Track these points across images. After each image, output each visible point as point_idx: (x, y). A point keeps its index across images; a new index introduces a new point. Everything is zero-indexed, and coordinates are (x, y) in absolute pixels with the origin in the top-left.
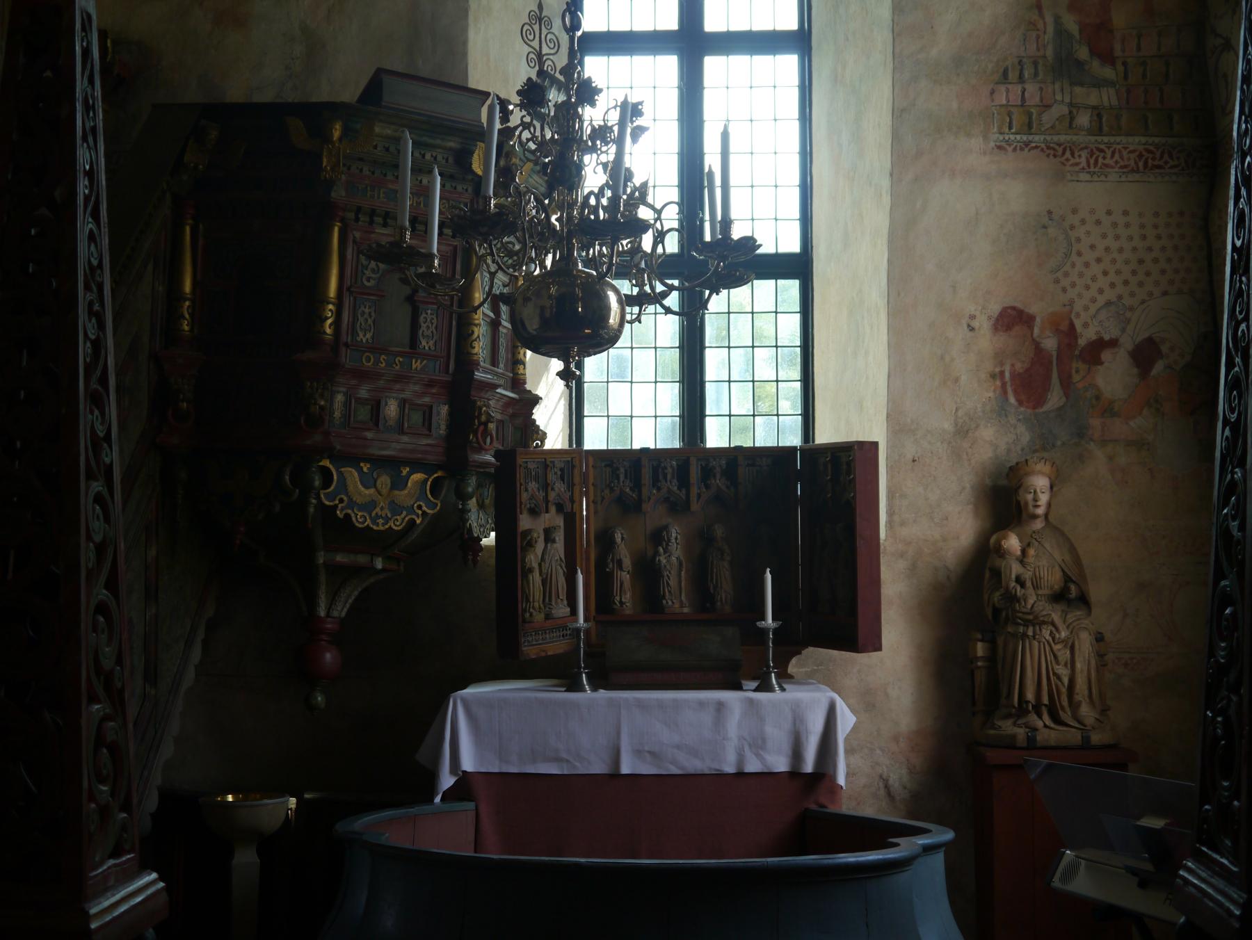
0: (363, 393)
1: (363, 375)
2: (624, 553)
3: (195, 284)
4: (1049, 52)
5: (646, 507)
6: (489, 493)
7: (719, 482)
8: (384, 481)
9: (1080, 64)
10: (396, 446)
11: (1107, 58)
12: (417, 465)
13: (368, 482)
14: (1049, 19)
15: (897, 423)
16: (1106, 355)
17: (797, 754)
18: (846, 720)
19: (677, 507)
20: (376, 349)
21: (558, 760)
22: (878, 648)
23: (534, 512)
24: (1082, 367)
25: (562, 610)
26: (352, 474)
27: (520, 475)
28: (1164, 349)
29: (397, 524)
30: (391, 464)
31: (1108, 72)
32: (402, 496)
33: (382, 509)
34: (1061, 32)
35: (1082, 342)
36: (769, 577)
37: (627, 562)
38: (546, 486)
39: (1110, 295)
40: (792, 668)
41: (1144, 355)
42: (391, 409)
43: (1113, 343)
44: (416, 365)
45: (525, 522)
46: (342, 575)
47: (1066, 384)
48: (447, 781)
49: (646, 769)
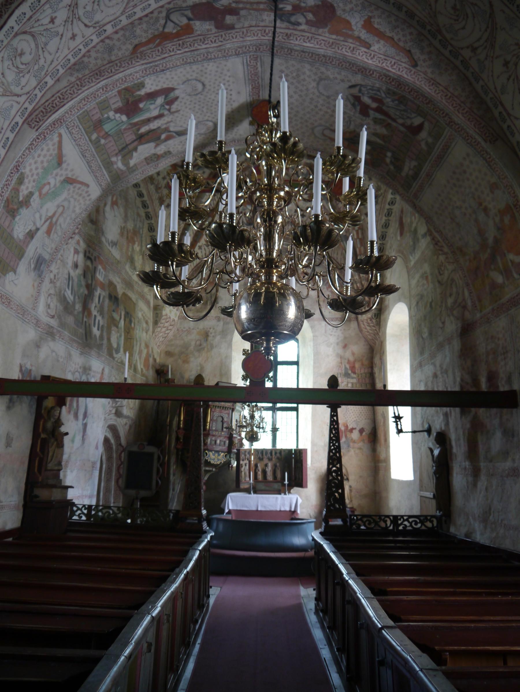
0: (213, 439)
1: (213, 436)
2: (260, 468)
3: (184, 418)
4: (343, 372)
5: (264, 459)
6: (235, 456)
7: (278, 455)
8: (216, 455)
9: (349, 374)
10: (219, 448)
11: (354, 373)
12: (222, 452)
13: (214, 455)
14: (343, 366)
15: (313, 444)
16: (354, 431)
17: (291, 507)
18: (300, 501)
19: (270, 459)
20: (216, 430)
21: (247, 507)
22: (306, 487)
23: (243, 460)
24: (349, 433)
25: (248, 479)
26: (211, 453)
27: (241, 453)
28: (365, 430)
29: (218, 463)
30: (218, 452)
31: (355, 376)
32: (220, 457)
33: (216, 460)
34: (346, 368)
35: (349, 428)
36: (286, 474)
37: (260, 470)
38: (245, 455)
39: (355, 419)
40: (292, 491)
41: (361, 431)
42: (218, 442)
43: (355, 429)
44: (223, 433)
45: (241, 462)
46: (207, 472)
47: (346, 436)
48: (227, 511)
49: (263, 509)
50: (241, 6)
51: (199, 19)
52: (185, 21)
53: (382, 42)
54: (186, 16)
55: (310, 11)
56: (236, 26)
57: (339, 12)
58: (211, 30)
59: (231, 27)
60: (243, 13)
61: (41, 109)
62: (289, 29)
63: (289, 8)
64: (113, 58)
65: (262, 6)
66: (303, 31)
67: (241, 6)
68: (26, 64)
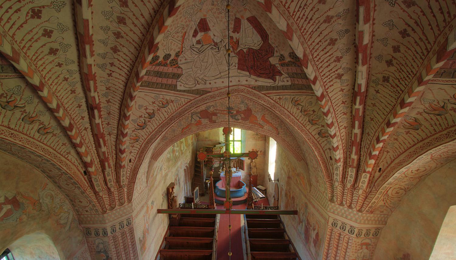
50: (218, 111)
51: (203, 118)
52: (198, 119)
53: (268, 125)
54: (198, 117)
55: (243, 113)
56: (217, 122)
57: (253, 113)
58: (207, 123)
59: (215, 122)
60: (218, 115)
61: (156, 154)
62: (235, 122)
63: (235, 112)
64: (176, 134)
65: (225, 112)
66: (240, 123)
67: (218, 111)
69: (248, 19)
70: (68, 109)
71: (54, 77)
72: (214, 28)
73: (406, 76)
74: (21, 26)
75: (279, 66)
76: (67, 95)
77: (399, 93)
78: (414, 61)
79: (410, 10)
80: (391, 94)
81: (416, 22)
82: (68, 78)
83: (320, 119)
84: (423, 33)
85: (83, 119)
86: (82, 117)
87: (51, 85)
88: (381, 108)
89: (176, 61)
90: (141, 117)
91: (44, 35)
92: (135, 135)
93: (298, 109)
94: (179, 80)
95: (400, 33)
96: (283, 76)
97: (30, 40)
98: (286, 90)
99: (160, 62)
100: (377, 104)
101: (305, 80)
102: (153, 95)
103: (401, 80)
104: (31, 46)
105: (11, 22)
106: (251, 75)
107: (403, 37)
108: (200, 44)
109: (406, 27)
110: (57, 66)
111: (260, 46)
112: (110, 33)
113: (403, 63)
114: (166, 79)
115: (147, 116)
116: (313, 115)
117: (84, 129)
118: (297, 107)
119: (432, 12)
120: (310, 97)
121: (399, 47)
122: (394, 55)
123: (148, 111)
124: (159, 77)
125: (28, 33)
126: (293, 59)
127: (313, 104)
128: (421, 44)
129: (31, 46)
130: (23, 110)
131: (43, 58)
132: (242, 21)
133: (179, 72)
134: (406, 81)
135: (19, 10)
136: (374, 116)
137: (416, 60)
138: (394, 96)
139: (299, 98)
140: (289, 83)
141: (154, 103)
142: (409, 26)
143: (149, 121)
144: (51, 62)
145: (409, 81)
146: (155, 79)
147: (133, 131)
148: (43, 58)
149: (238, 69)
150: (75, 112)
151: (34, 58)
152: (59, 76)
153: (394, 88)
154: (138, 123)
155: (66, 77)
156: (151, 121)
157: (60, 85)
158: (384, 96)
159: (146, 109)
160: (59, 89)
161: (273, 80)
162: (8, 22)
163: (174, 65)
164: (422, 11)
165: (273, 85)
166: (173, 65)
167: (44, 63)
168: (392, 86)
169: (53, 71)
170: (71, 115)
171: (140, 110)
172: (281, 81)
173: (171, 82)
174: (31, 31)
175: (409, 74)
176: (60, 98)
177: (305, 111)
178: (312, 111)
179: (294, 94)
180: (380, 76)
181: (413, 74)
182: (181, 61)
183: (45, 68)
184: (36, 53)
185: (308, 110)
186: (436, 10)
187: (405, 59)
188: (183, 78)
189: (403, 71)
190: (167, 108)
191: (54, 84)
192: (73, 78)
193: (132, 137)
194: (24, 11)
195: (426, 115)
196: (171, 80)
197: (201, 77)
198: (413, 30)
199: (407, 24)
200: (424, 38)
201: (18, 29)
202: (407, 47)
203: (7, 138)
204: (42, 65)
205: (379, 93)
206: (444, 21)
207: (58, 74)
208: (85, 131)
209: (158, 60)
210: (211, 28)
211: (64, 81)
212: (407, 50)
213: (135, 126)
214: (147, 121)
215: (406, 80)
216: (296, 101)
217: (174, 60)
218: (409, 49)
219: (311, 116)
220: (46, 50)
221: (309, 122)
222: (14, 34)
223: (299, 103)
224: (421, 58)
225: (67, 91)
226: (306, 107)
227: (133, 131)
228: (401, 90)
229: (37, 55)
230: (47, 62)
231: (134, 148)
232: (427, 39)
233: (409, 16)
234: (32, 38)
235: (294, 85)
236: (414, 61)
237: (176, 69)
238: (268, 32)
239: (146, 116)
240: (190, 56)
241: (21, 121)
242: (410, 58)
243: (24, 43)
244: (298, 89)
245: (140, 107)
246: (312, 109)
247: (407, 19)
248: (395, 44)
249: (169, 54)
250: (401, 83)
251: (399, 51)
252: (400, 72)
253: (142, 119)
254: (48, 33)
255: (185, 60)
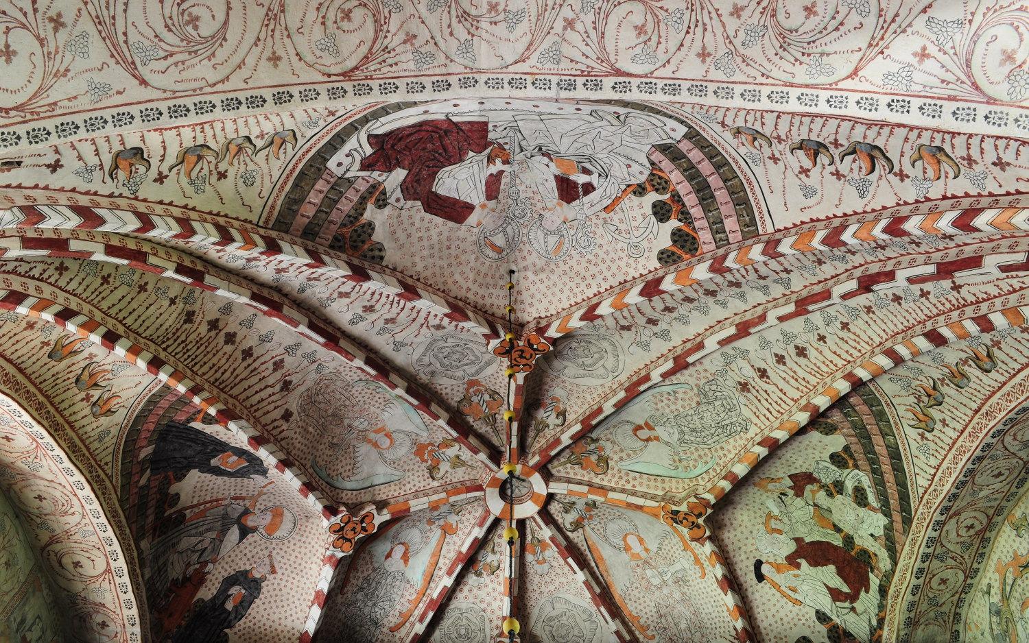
68: (1017, 28)
69: (470, 208)
70: (906, 324)
71: (846, 347)
72: (545, 177)
73: (190, 353)
74: (781, 390)
75: (380, 179)
76: (879, 322)
77: (164, 342)
78: (211, 368)
79: (270, 365)
80: (164, 328)
81: (255, 369)
82: (841, 323)
83: (192, 183)
84: (242, 380)
85: (929, 293)
86: (922, 296)
87: (860, 351)
88: (134, 305)
89: (652, 180)
90: (838, 175)
91: (784, 364)
92: (919, 164)
93: (262, 136)
94: (670, 141)
95: (251, 348)
96: (357, 165)
97: (796, 380)
98: (329, 142)
99: (680, 220)
100: (143, 295)
101: (311, 214)
102: (758, 171)
103: (183, 345)
104: (804, 379)
105: (780, 402)
106: (445, 118)
107: (243, 352)
108: (583, 167)
109: (255, 356)
110: (825, 342)
111: (437, 180)
112: (720, 297)
113: (208, 349)
114: (699, 166)
115: (823, 159)
116: (212, 167)
117: (955, 293)
118: (266, 137)
119: (261, 390)
120: (265, 194)
121: (233, 343)
122: (223, 333)
123: (807, 163)
124: (709, 187)
125: (788, 382)
126: (363, 226)
127: (242, 187)
128: (232, 379)
129: (804, 379)
130: (939, 382)
131: (815, 365)
132: (482, 198)
133: (657, 156)
134: (181, 354)
135: (766, 391)
136: (115, 288)
137: (213, 371)
138: (159, 333)
139: (282, 156)
140: (332, 164)
141: (775, 160)
142: (254, 361)
143: (836, 144)
144: (821, 353)
145: (182, 360)
146: (721, 195)
147: (902, 176)
148: (815, 365)
149: (486, 124)
150: (911, 310)
151: (818, 375)
152: (842, 339)
153: (174, 334)
154: (864, 171)
155: (840, 326)
156: (832, 139)
157: (858, 336)
158: (161, 314)
159: (805, 171)
160: (867, 339)
161: (376, 136)
162: (780, 405)
163: (660, 178)
164: (264, 377)
165: (370, 124)
166: (663, 181)
167: (824, 363)
168: (178, 329)
169: (834, 348)
170: (918, 319)
171: (818, 187)
172: (355, 150)
173: (694, 151)
174: (784, 379)
175: (193, 360)
176: (885, 337)
177: (240, 149)
178: (226, 171)
179: (301, 152)
180: (196, 307)
181: (193, 366)
182: (640, 175)
183: (831, 362)
184: (810, 373)
185: (235, 162)
186: (263, 395)
187: (214, 351)
188: (656, 140)
189: (198, 348)
190: (750, 125)
191: (859, 347)
192: (838, 314)
193: (931, 173)
194: (766, 387)
195: (83, 364)
196: (690, 156)
197: (604, 123)
198: (249, 365)
199: (258, 358)
200: (239, 378)
201: (785, 394)
202: (230, 356)
203: (989, 427)
204: (827, 366)
205: (170, 305)
206: (252, 406)
207: (838, 340)
208: (964, 291)
209: (680, 230)
210: (553, 178)
211: (849, 330)
212: (227, 356)
213: (880, 178)
214: (841, 149)
215: (184, 353)
216: (284, 142)
217: (653, 186)
218: (228, 359)
219: (214, 162)
220: (802, 361)
221: (202, 146)
222: (792, 399)
223: (274, 148)
224: (216, 380)
225: (870, 322)
226: (247, 159)
227: (902, 176)
228: (168, 346)
229: (813, 373)
230: (822, 358)
231: (975, 154)
232: (235, 385)
233: (265, 362)
234: (793, 377)
235: (319, 170)
236: (211, 368)
237: (662, 165)
238: (428, 216)
239: (826, 161)
240: (615, 163)
241: (962, 390)
242: (215, 360)
243: (801, 388)
244: (302, 173)
245: (808, 192)
246: (231, 174)
247: (262, 360)
248: (238, 339)
249: (655, 214)
250: (179, 345)
251: (226, 342)
252: (197, 342)
253: (844, 167)
254: (780, 359)
255: (630, 166)
